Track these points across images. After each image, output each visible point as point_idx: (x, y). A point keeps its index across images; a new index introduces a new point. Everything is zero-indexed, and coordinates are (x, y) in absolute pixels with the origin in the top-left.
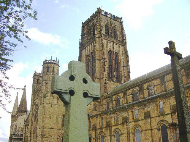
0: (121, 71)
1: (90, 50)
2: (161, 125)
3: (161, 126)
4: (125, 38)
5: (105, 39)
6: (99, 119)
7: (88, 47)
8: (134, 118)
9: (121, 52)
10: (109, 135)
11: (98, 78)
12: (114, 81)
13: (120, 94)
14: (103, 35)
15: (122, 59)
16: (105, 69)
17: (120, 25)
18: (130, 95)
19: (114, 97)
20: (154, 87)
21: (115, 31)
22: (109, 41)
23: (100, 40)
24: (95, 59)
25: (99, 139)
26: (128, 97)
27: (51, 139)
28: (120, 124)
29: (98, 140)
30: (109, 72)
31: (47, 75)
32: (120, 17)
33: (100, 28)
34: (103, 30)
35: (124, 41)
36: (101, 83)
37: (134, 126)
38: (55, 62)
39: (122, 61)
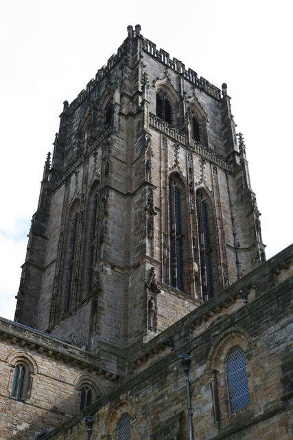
0: (226, 266)
11: (113, 267)
15: (229, 222)
17: (217, 110)
22: (173, 140)
23: (135, 125)
24: (108, 188)
28: (268, 415)
30: (168, 253)
33: (137, 87)
36: (126, 290)
39: (228, 228)
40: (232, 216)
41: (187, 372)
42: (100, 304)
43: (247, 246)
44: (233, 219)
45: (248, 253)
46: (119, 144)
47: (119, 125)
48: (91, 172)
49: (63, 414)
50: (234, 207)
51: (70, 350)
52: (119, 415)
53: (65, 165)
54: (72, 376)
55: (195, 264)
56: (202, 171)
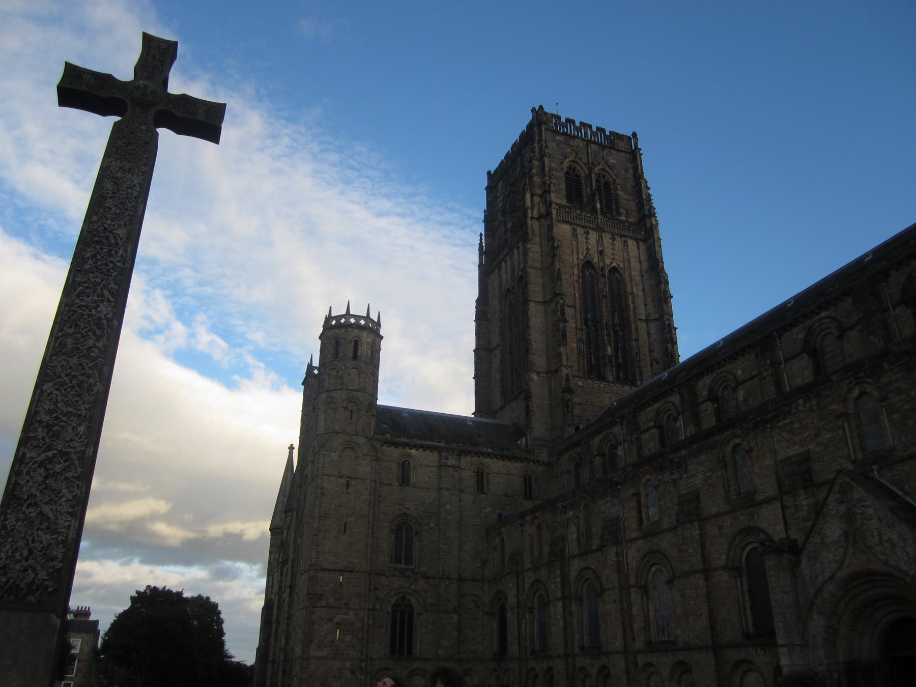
0: (637, 340)
1: (513, 271)
2: (746, 552)
3: (744, 558)
4: (651, 208)
5: (566, 222)
6: (530, 530)
7: (508, 258)
8: (645, 523)
9: (635, 264)
10: (559, 594)
11: (538, 373)
12: (608, 381)
13: (617, 429)
14: (554, 205)
15: (641, 293)
16: (564, 337)
18: (649, 429)
19: (597, 440)
20: (735, 390)
21: (606, 190)
22: (584, 227)
25: (531, 610)
26: (646, 436)
27: (346, 613)
28: (597, 550)
29: (527, 616)
31: (334, 373)
32: (625, 131)
34: (552, 188)
35: (645, 224)
37: (645, 555)
38: (362, 322)
39: (640, 301)
40: (643, 288)
41: (565, 513)
42: (531, 408)
43: (657, 316)
44: (644, 290)
45: (658, 322)
46: (535, 250)
47: (532, 231)
48: (516, 264)
49: (512, 496)
50: (646, 277)
51: (512, 451)
52: (536, 523)
53: (496, 243)
54: (516, 467)
55: (609, 348)
56: (613, 249)
